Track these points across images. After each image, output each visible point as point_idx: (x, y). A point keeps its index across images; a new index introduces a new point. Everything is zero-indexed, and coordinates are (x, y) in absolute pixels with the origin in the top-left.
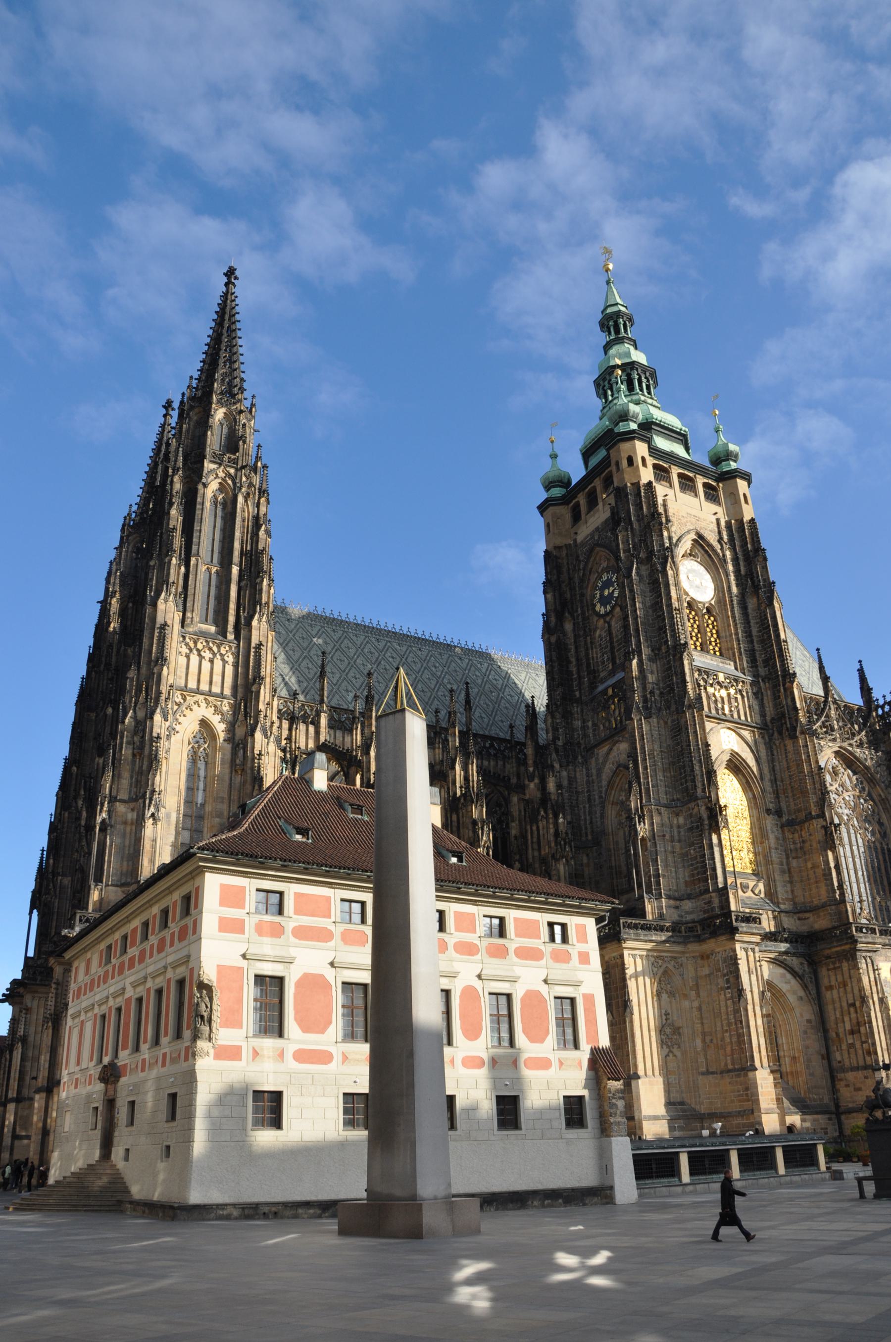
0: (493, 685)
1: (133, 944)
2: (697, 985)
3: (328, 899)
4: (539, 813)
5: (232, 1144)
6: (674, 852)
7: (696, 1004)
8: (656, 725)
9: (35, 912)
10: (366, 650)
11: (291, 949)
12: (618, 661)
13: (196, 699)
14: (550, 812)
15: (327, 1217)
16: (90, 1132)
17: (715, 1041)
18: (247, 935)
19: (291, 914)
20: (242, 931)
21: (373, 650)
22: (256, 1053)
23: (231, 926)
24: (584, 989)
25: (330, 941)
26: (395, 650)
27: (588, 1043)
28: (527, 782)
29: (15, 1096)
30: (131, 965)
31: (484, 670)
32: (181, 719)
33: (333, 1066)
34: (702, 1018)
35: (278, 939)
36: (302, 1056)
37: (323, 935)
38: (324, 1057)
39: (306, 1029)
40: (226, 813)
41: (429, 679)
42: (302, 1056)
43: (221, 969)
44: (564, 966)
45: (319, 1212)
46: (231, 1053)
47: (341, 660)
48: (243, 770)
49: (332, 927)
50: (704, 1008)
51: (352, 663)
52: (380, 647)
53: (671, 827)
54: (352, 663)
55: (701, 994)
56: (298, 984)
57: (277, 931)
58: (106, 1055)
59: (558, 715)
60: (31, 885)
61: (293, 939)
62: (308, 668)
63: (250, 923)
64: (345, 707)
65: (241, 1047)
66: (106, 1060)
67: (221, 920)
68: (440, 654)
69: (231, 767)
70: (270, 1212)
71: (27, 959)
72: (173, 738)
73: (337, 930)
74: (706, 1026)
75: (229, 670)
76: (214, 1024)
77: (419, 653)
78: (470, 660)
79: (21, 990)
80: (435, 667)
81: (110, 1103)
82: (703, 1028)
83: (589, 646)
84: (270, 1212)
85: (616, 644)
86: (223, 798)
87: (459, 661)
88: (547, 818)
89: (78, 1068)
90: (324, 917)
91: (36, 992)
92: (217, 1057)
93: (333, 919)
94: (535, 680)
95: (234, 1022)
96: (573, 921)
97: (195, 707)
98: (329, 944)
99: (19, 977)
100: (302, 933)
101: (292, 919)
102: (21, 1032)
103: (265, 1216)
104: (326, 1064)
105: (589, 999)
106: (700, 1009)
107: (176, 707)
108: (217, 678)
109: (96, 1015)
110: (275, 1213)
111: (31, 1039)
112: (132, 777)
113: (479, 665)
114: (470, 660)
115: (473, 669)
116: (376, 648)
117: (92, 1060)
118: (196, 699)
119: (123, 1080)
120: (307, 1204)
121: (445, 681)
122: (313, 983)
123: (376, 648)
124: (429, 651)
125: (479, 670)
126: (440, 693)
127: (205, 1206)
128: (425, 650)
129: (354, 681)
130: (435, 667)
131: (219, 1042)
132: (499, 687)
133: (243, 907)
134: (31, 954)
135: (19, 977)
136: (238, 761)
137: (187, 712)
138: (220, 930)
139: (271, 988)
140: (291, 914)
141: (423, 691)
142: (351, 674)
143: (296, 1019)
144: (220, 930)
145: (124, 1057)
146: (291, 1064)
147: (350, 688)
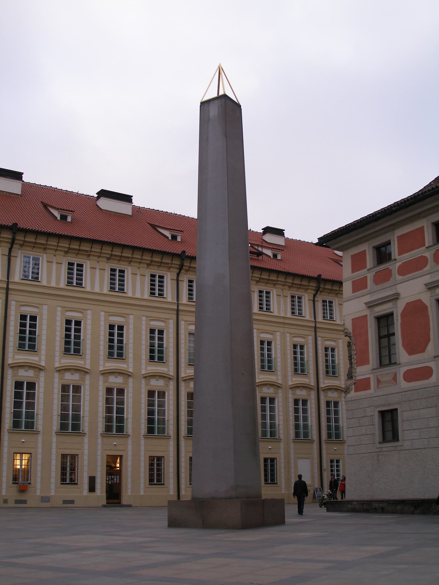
15: (417, 514)
20: (365, 287)
22: (379, 381)
23: (359, 285)
25: (425, 266)
35: (388, 282)
36: (410, 376)
38: (426, 373)
39: (411, 352)
46: (364, 385)
56: (403, 315)
61: (399, 278)
65: (369, 378)
92: (356, 391)
95: (364, 361)
100: (405, 270)
101: (399, 259)
103: (376, 511)
104: (428, 379)
110: (383, 509)
131: (358, 378)
143: (403, 345)
146: (403, 384)
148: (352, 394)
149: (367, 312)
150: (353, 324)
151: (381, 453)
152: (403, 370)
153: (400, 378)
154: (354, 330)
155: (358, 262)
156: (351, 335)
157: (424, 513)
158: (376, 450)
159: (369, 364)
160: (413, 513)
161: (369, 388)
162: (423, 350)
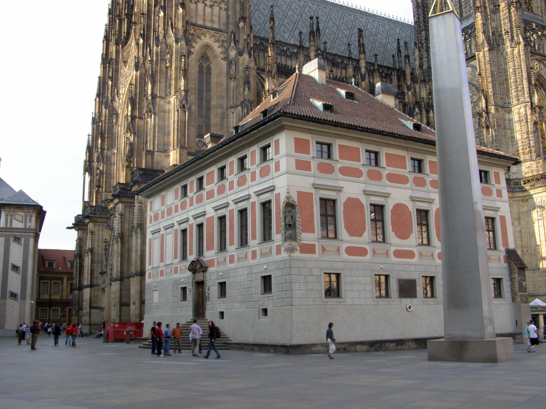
0: (370, 32)
1: (210, 182)
2: (519, 217)
3: (358, 149)
4: (414, 111)
5: (315, 307)
6: (506, 136)
7: (518, 229)
8: (496, 55)
9: (87, 173)
10: (293, 7)
11: (340, 182)
12: (464, 15)
13: (202, 32)
14: (424, 109)
15: (373, 351)
16: (180, 302)
17: (530, 251)
18: (313, 172)
19: (338, 159)
20: (309, 169)
21: (297, 7)
22: (324, 249)
23: (303, 166)
24: (500, 213)
26: (310, 7)
27: (503, 246)
28: (406, 91)
29: (89, 283)
30: (210, 195)
31: (364, 22)
32: (194, 44)
33: (368, 257)
34: (521, 237)
37: (356, 173)
38: (362, 252)
39: (351, 234)
40: (225, 106)
41: (332, 26)
42: (351, 251)
43: (299, 194)
44: (489, 198)
45: (368, 347)
46: (309, 249)
47: (278, 13)
48: (235, 78)
49: (362, 169)
50: (523, 231)
51: (285, 14)
52: (301, 5)
53: (505, 120)
54: (285, 14)
55: (522, 223)
56: (345, 204)
57: (329, 170)
58: (191, 253)
59: (422, 50)
60: (82, 156)
62: (259, 17)
63: (314, 164)
64: (284, 41)
65: (315, 245)
66: (191, 258)
67: (297, 161)
68: (337, 11)
69: (227, 76)
70: (341, 348)
71: (85, 202)
72: (190, 59)
73: (364, 170)
74: (524, 242)
75: (223, 13)
76: (298, 231)
77: (325, 10)
78: (355, 16)
79: (87, 221)
80: (335, 19)
81: (200, 284)
82: (522, 244)
83: (443, 5)
84: (341, 348)
85: (463, 4)
86: (223, 96)
87: (349, 16)
88: (421, 113)
89: (162, 264)
90: (356, 161)
91: (96, 222)
92: (301, 252)
93: (362, 163)
94: (395, 30)
96: (493, 171)
97: (202, 37)
98: (361, 179)
99: (81, 213)
100: (345, 171)
102: (89, 245)
104: (364, 256)
105: (503, 218)
106: (520, 232)
107: (190, 37)
108: (216, 19)
109: (176, 230)
110: (344, 349)
111: (96, 250)
112: (166, 82)
113: (361, 19)
114: (355, 16)
115: (357, 21)
116: (299, 6)
117: (176, 257)
118: (202, 32)
119: (210, 269)
120: (362, 343)
121: (342, 28)
122: (353, 204)
123: (299, 6)
124: (331, 9)
125: (360, 22)
126: (340, 36)
127: (304, 345)
128: (328, 8)
129: (288, 26)
130: (335, 19)
132: (374, 33)
133: (309, 154)
134: (86, 199)
135: (81, 213)
136: (232, 73)
137: (198, 40)
138: (297, 169)
139: (328, 206)
140: (338, 159)
141: (329, 34)
142: (286, 22)
143: (345, 227)
144: (297, 169)
145: (209, 255)
147: (286, 31)
148: (297, 254)
149: (313, 191)
150: (298, 196)
151: (327, 306)
152: (344, 246)
153: (343, 250)
154: (298, 200)
155: (301, 146)
156: (297, 204)
157: (376, 350)
158: (323, 303)
159: (314, 232)
160: (368, 351)
161: (315, 253)
162: (360, 235)
